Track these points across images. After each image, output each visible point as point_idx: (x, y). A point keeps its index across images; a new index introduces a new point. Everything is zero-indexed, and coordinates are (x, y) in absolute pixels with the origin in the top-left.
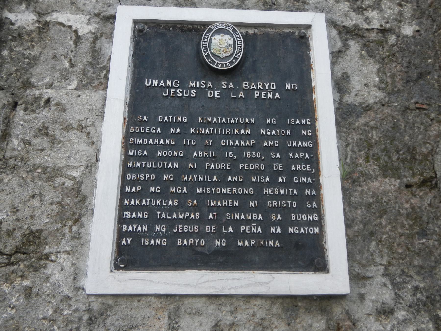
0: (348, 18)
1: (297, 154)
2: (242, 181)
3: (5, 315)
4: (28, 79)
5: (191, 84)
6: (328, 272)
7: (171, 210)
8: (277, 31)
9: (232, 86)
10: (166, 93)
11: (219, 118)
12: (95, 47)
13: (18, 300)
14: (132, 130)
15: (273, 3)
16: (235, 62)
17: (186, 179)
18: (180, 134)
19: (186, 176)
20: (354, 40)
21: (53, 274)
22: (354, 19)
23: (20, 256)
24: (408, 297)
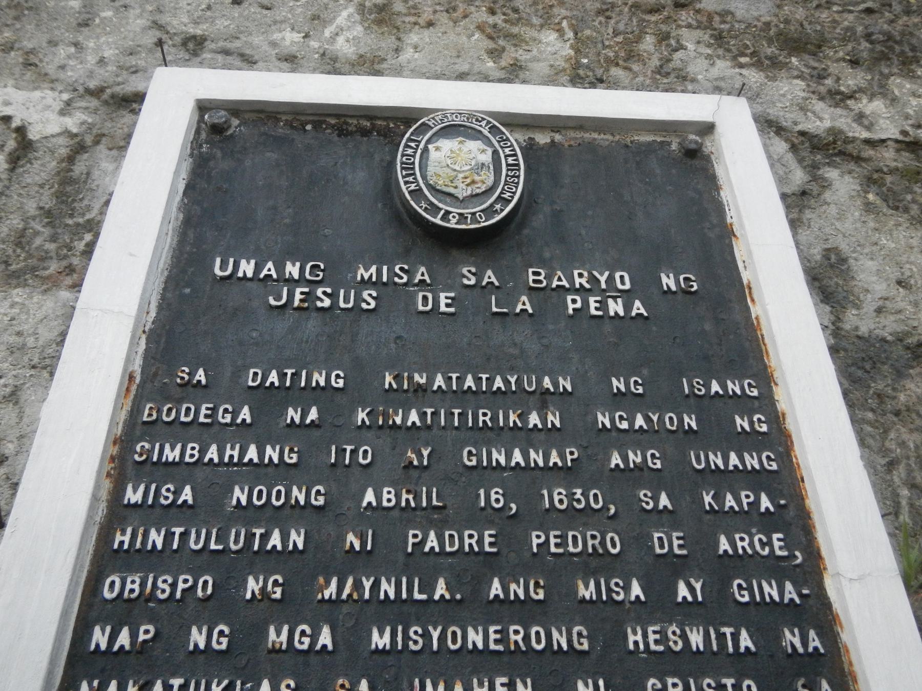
0: (809, 114)
1: (729, 497)
2: (541, 596)
5: (361, 271)
8: (617, 137)
9: (493, 279)
10: (278, 298)
11: (454, 376)
12: (72, 170)
14: (150, 415)
15: (597, 79)
16: (502, 210)
17: (330, 591)
18: (318, 426)
19: (334, 582)
20: (835, 167)
22: (826, 116)
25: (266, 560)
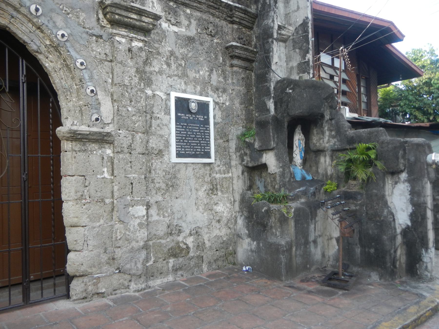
7: (185, 145)
24: (222, 163)
25: (184, 137)
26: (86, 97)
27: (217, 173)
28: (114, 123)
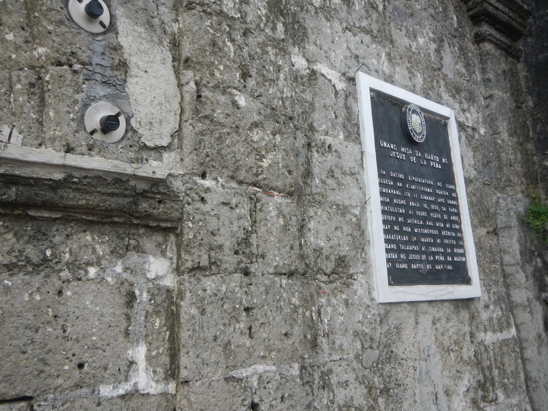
3: (339, 321)
4: (312, 123)
6: (471, 284)
13: (343, 309)
21: (358, 289)
23: (336, 276)
26: (63, 29)
27: (485, 331)
28: (180, 147)
